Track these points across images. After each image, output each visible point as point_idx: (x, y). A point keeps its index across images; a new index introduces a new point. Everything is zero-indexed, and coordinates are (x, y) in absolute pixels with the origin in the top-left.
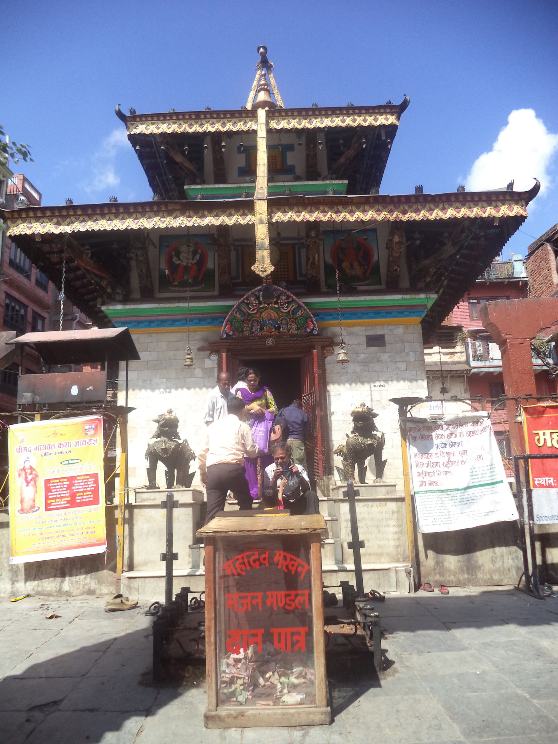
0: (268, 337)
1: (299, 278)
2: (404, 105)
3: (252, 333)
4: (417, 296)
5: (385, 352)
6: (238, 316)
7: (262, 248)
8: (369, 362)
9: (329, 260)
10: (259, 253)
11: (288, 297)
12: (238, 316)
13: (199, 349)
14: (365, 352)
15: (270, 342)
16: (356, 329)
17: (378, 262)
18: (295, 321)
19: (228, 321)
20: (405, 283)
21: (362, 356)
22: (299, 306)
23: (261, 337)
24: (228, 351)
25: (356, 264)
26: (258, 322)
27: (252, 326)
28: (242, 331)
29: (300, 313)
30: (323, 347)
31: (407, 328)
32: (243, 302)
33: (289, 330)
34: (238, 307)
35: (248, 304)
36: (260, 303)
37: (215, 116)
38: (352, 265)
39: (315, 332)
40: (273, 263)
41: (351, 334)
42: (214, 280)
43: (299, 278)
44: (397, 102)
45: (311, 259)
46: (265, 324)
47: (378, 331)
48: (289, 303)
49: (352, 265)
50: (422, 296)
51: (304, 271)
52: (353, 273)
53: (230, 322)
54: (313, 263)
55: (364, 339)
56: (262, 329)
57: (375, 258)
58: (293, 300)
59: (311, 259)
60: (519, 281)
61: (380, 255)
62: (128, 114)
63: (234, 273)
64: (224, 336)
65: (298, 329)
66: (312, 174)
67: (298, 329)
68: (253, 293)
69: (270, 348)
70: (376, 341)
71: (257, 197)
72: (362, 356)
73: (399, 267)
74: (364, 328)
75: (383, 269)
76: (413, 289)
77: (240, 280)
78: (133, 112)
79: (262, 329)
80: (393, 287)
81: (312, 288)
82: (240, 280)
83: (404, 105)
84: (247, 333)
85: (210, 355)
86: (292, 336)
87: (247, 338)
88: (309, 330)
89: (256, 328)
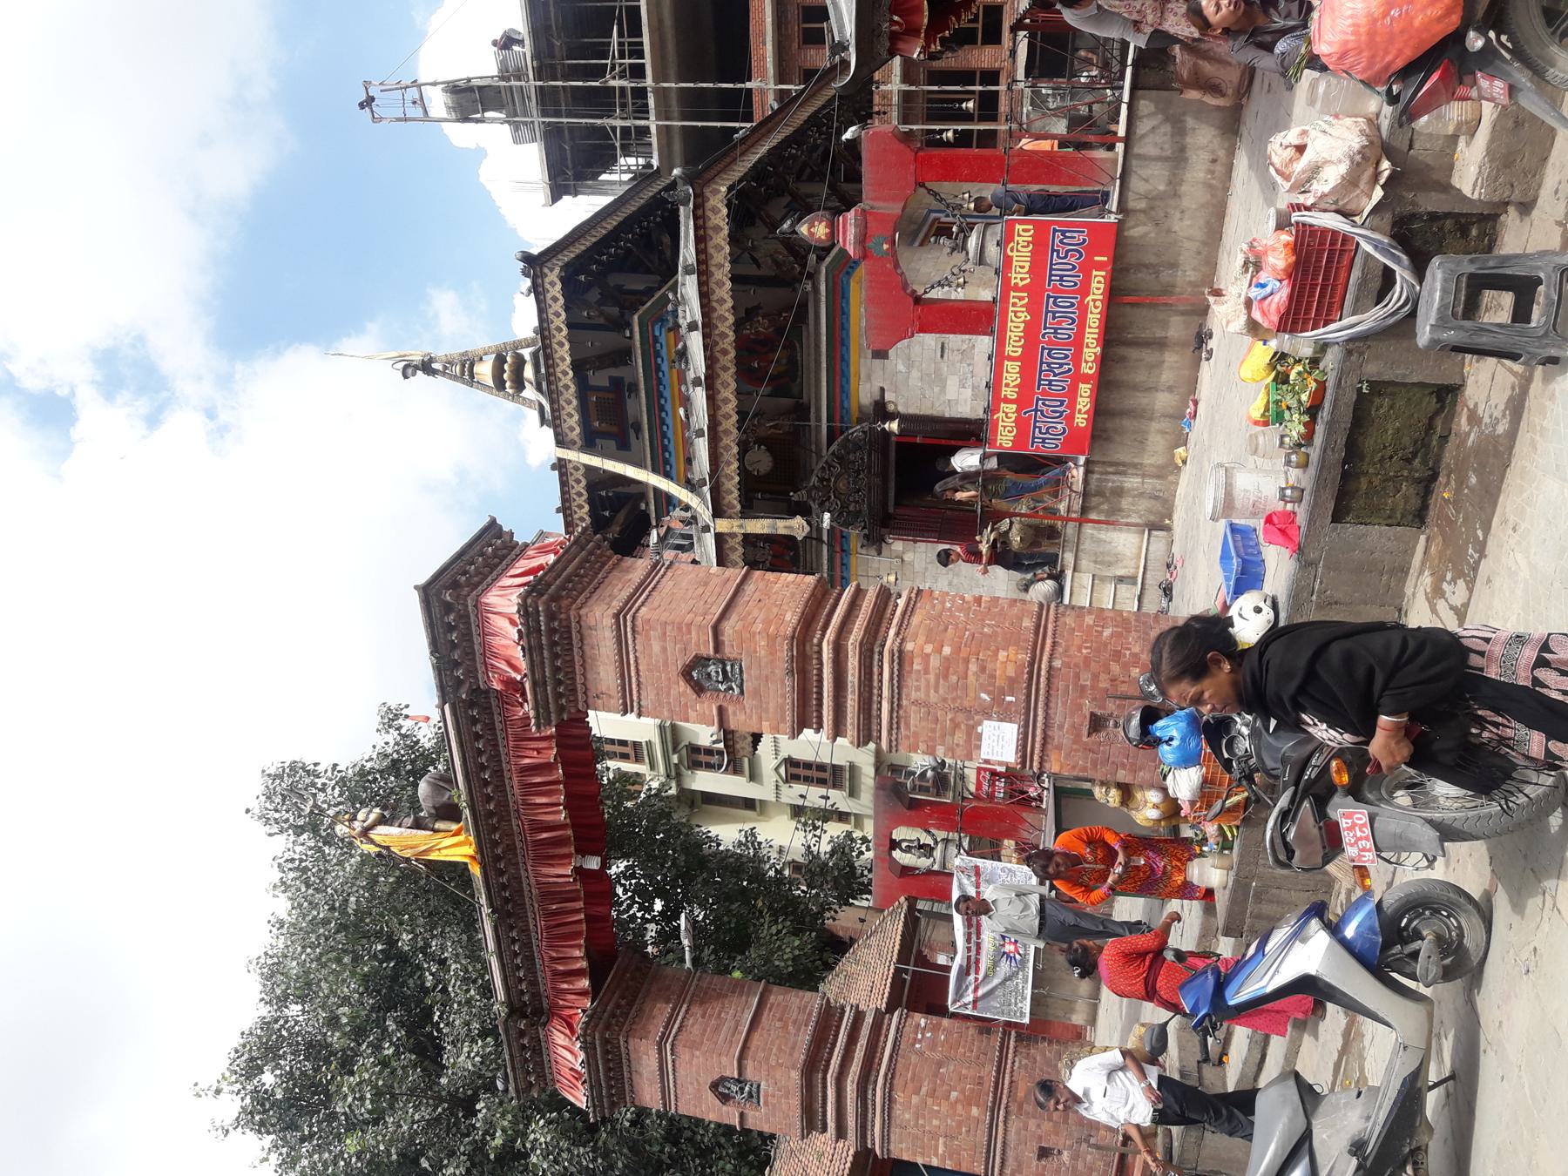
10: (781, 532)
13: (879, 553)
21: (901, 367)
41: (869, 377)
53: (847, 525)
55: (878, 362)
66: (624, 356)
72: (901, 367)
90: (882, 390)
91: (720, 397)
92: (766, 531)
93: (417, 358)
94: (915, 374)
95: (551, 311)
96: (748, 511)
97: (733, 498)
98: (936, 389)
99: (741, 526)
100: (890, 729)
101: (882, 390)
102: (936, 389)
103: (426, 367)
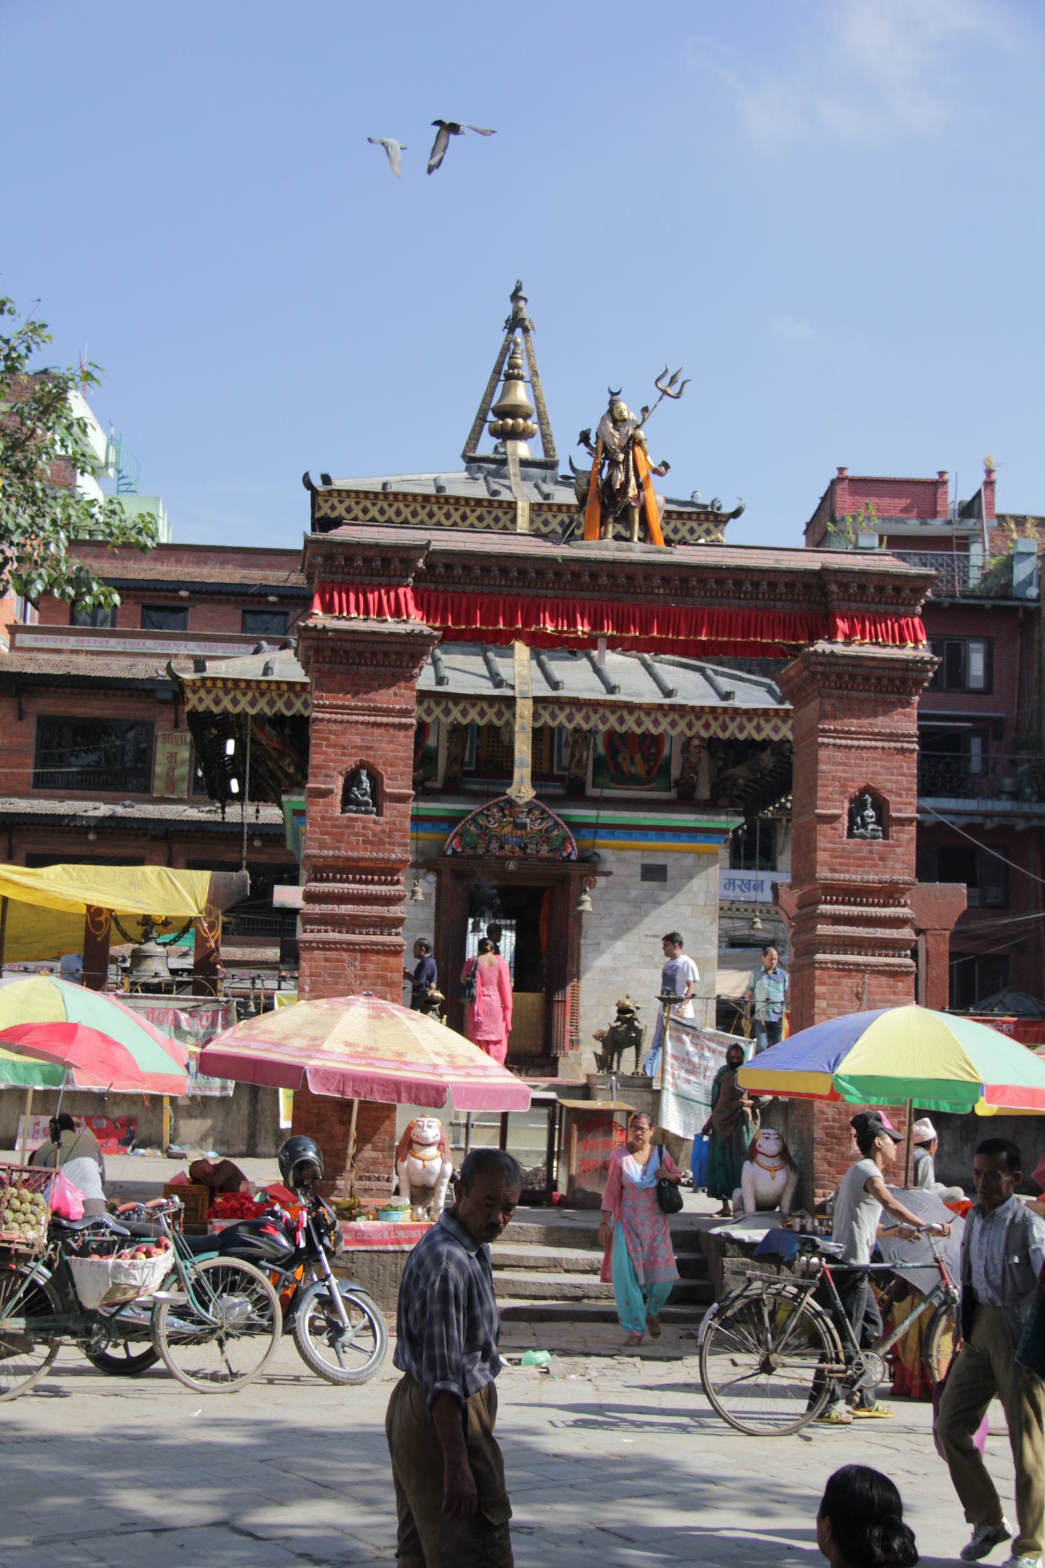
0: (507, 858)
1: (555, 772)
2: (736, 514)
3: (487, 851)
4: (717, 818)
5: (665, 889)
6: (472, 828)
7: (522, 764)
8: (643, 902)
9: (601, 750)
10: (517, 774)
11: (543, 812)
12: (472, 828)
14: (639, 888)
15: (512, 866)
16: (628, 854)
17: (670, 757)
18: (547, 841)
19: (456, 834)
20: (704, 792)
22: (556, 824)
23: (498, 858)
24: (452, 871)
25: (638, 757)
26: (498, 838)
27: (490, 843)
28: (475, 848)
29: (556, 833)
30: (582, 877)
31: (699, 858)
32: (481, 813)
33: (538, 852)
34: (474, 819)
35: (487, 816)
36: (504, 816)
37: (452, 501)
38: (632, 758)
39: (573, 857)
40: (534, 786)
41: (622, 860)
42: (436, 764)
43: (555, 772)
44: (727, 509)
45: (578, 757)
46: (507, 842)
47: (659, 860)
48: (543, 819)
49: (632, 758)
50: (723, 818)
51: (565, 763)
52: (633, 770)
54: (580, 761)
55: (638, 870)
56: (501, 847)
57: (666, 752)
58: (550, 816)
59: (578, 757)
60: (1016, 608)
61: (672, 750)
62: (317, 482)
63: (467, 759)
64: (449, 852)
65: (551, 851)
67: (551, 851)
68: (497, 804)
69: (511, 872)
70: (654, 873)
71: (521, 692)
72: (633, 893)
73: (696, 773)
74: (639, 853)
75: (675, 772)
76: (711, 806)
77: (473, 768)
78: (326, 479)
79: (501, 847)
80: (686, 800)
81: (576, 794)
82: (473, 768)
83: (736, 514)
84: (480, 851)
85: (426, 874)
86: (542, 859)
87: (481, 857)
88: (565, 854)
89: (494, 845)
90: (608, 874)
91: (659, 716)
92: (517, 755)
93: (527, 312)
94: (627, 909)
95: (679, 523)
96: (539, 735)
97: (546, 717)
98: (610, 931)
99: (523, 728)
100: (838, 963)
101: (608, 874)
102: (610, 931)
103: (515, 322)
